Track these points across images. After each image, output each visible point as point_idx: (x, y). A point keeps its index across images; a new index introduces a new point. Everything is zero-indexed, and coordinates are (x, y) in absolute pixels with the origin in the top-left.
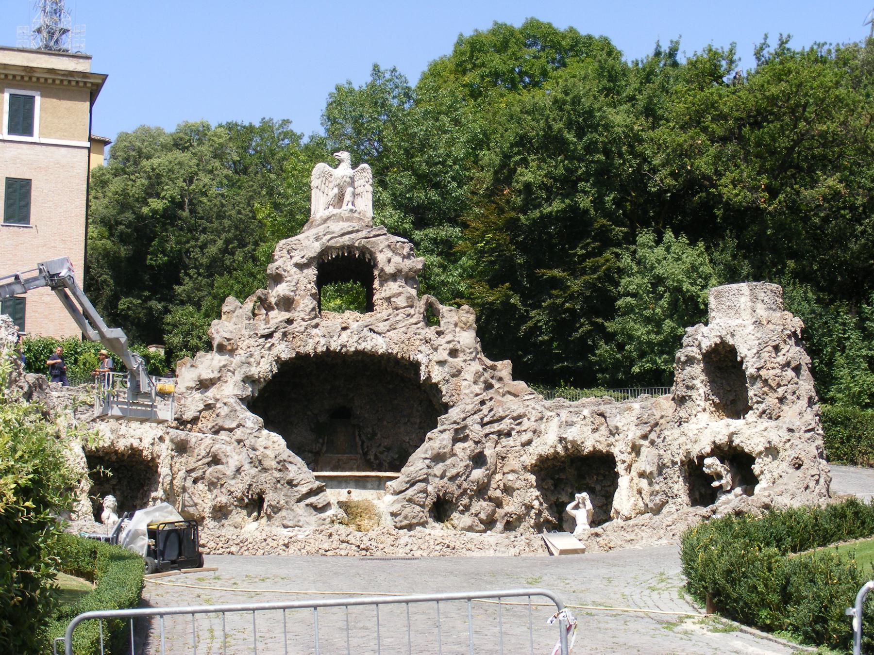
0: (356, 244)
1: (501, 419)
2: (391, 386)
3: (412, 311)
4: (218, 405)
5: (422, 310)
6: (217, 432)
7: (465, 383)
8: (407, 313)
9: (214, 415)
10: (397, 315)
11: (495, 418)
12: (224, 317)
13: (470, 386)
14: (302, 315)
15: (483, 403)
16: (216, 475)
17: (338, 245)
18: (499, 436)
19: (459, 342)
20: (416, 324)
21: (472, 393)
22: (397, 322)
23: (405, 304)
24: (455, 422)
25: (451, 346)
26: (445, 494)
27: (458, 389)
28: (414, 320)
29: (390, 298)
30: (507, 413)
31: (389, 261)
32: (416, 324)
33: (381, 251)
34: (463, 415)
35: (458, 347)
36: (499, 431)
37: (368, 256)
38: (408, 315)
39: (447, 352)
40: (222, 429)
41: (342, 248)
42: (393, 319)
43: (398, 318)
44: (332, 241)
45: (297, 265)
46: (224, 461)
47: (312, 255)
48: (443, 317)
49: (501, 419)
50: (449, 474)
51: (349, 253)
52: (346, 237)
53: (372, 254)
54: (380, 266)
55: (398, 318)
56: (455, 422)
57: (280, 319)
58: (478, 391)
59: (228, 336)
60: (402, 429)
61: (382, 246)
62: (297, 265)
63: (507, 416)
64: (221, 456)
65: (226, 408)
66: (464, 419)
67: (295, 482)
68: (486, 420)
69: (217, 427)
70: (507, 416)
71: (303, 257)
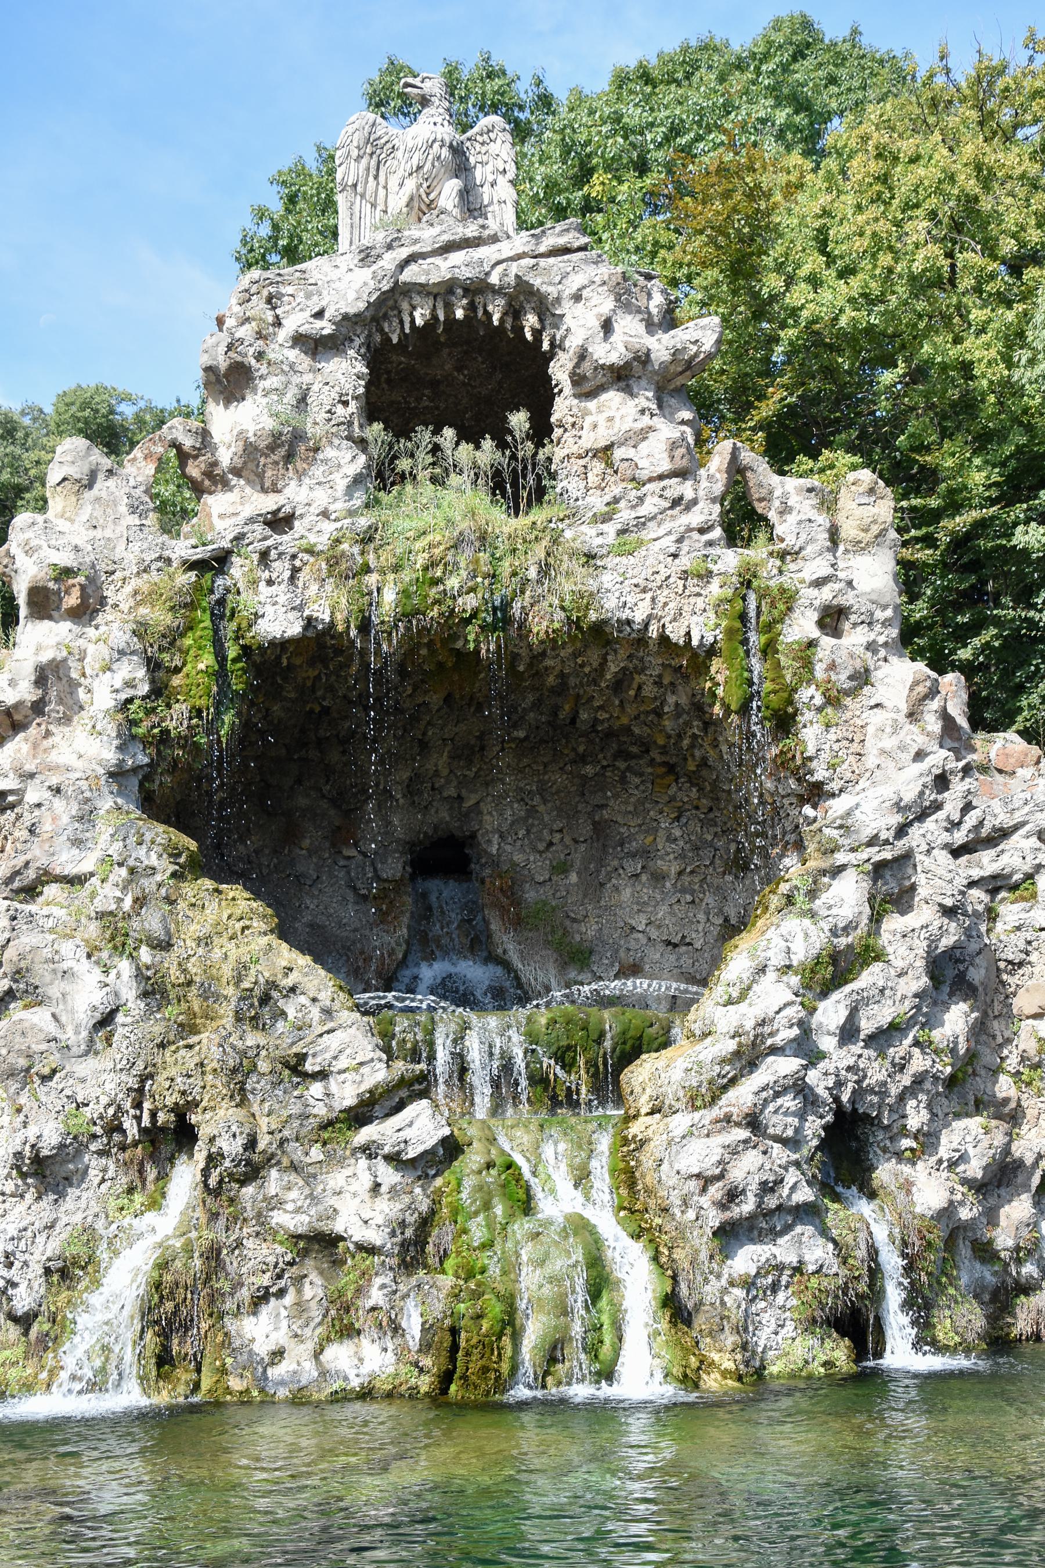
0: (494, 279)
1: (1003, 834)
2: (589, 770)
3: (687, 489)
4: (31, 796)
5: (719, 488)
6: (30, 892)
7: (877, 718)
8: (672, 493)
9: (24, 834)
10: (641, 499)
11: (984, 832)
12: (56, 504)
13: (896, 729)
14: (321, 498)
15: (942, 782)
16: (19, 1043)
17: (434, 279)
18: (993, 892)
19: (850, 583)
20: (702, 531)
21: (902, 748)
22: (642, 523)
23: (665, 466)
24: (872, 842)
25: (826, 594)
26: (858, 1093)
27: (855, 740)
28: (696, 518)
29: (609, 448)
30: (1018, 817)
31: (607, 326)
32: (702, 531)
33: (577, 297)
34: (896, 819)
35: (848, 599)
36: (994, 877)
37: (531, 320)
38: (676, 502)
39: (815, 617)
40: (47, 877)
41: (445, 291)
42: (625, 515)
43: (642, 511)
44: (413, 268)
45: (299, 340)
46: (54, 991)
47: (352, 310)
48: (785, 510)
49: (1003, 834)
50: (867, 1027)
51: (471, 307)
52: (457, 258)
53: (545, 308)
54: (573, 343)
55: (642, 511)
56: (873, 841)
57: (248, 511)
58: (921, 741)
59: (65, 559)
60: (627, 894)
61: (575, 282)
62: (299, 340)
63: (1016, 828)
64: (41, 974)
65: (59, 804)
66: (901, 831)
67: (309, 1066)
68: (960, 837)
69: (31, 874)
70: (1023, 824)
71: (319, 315)
